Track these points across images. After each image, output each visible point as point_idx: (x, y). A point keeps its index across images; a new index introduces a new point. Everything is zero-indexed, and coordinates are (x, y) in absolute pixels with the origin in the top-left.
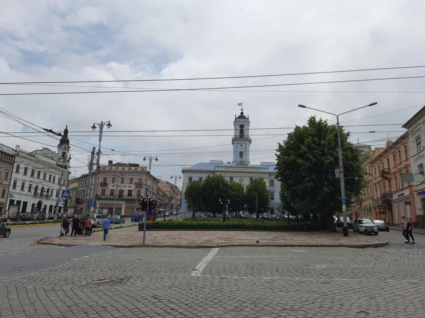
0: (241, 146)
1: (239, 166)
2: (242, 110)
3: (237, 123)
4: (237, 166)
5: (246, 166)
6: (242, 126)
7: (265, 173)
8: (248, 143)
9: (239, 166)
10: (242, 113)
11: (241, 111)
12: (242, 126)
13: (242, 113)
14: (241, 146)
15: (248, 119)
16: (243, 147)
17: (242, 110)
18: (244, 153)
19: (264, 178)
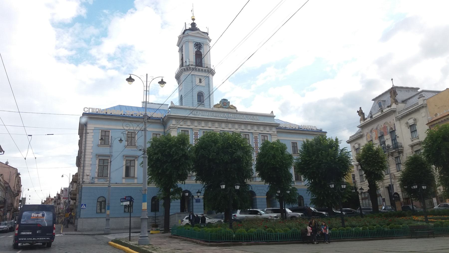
0: (200, 81)
1: (221, 109)
2: (193, 19)
3: (190, 38)
4: (216, 109)
5: (234, 111)
6: (198, 46)
7: (271, 126)
8: (211, 76)
9: (221, 109)
10: (193, 25)
11: (192, 22)
12: (198, 46)
13: (193, 25)
14: (200, 81)
15: (207, 34)
16: (203, 84)
17: (193, 19)
18: (206, 96)
19: (268, 135)
